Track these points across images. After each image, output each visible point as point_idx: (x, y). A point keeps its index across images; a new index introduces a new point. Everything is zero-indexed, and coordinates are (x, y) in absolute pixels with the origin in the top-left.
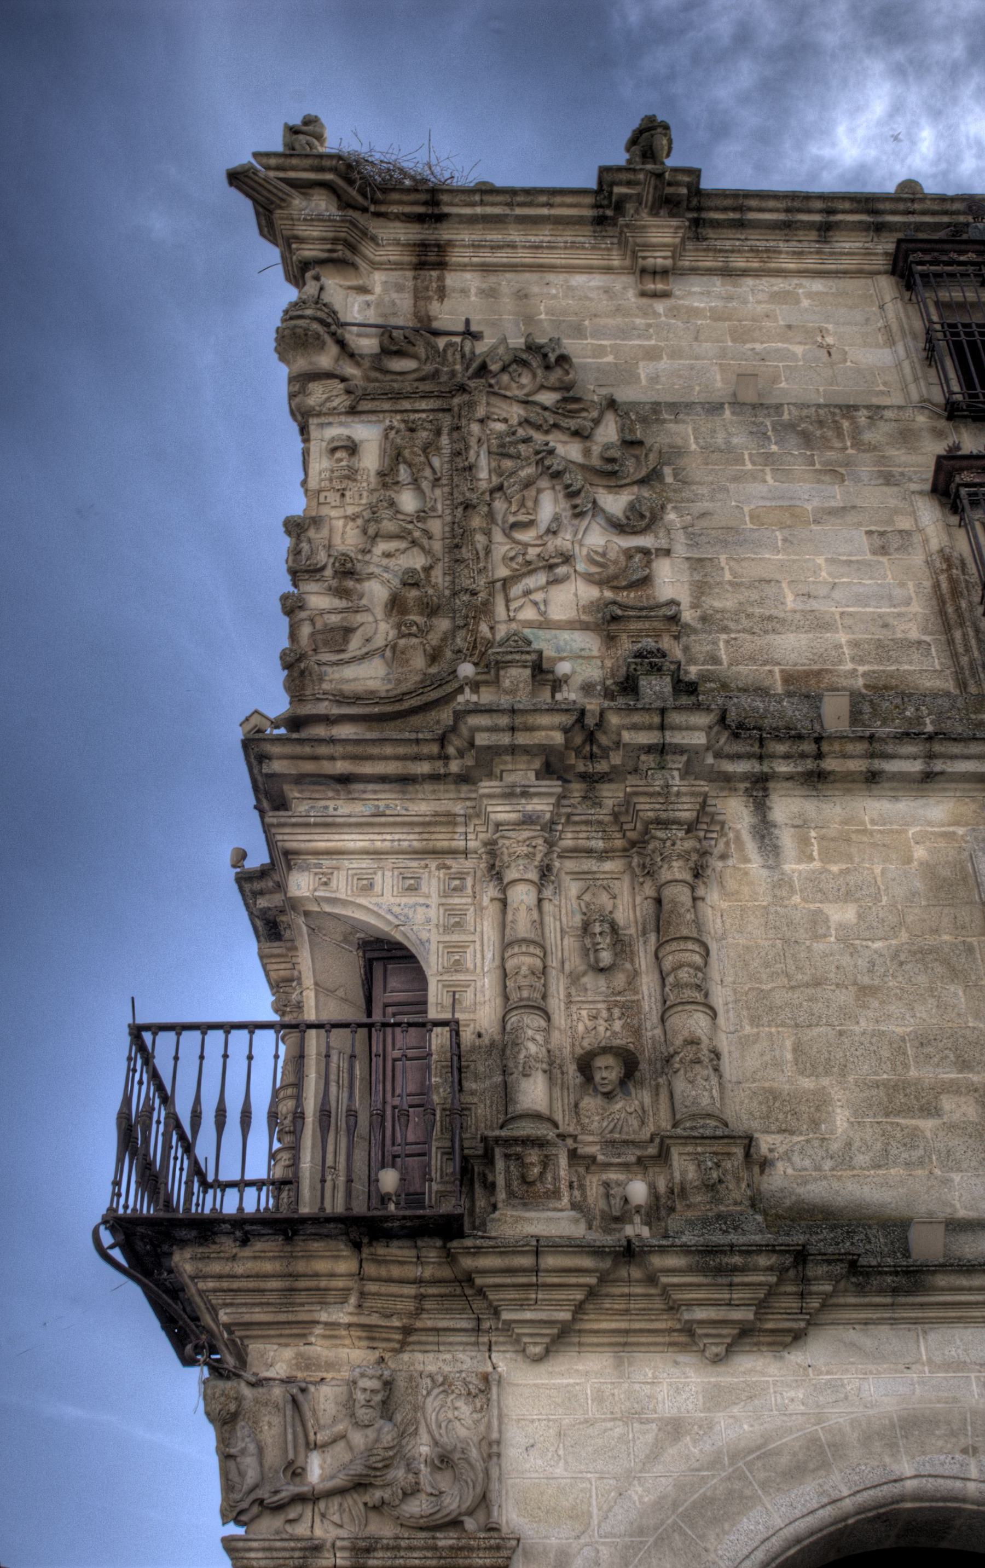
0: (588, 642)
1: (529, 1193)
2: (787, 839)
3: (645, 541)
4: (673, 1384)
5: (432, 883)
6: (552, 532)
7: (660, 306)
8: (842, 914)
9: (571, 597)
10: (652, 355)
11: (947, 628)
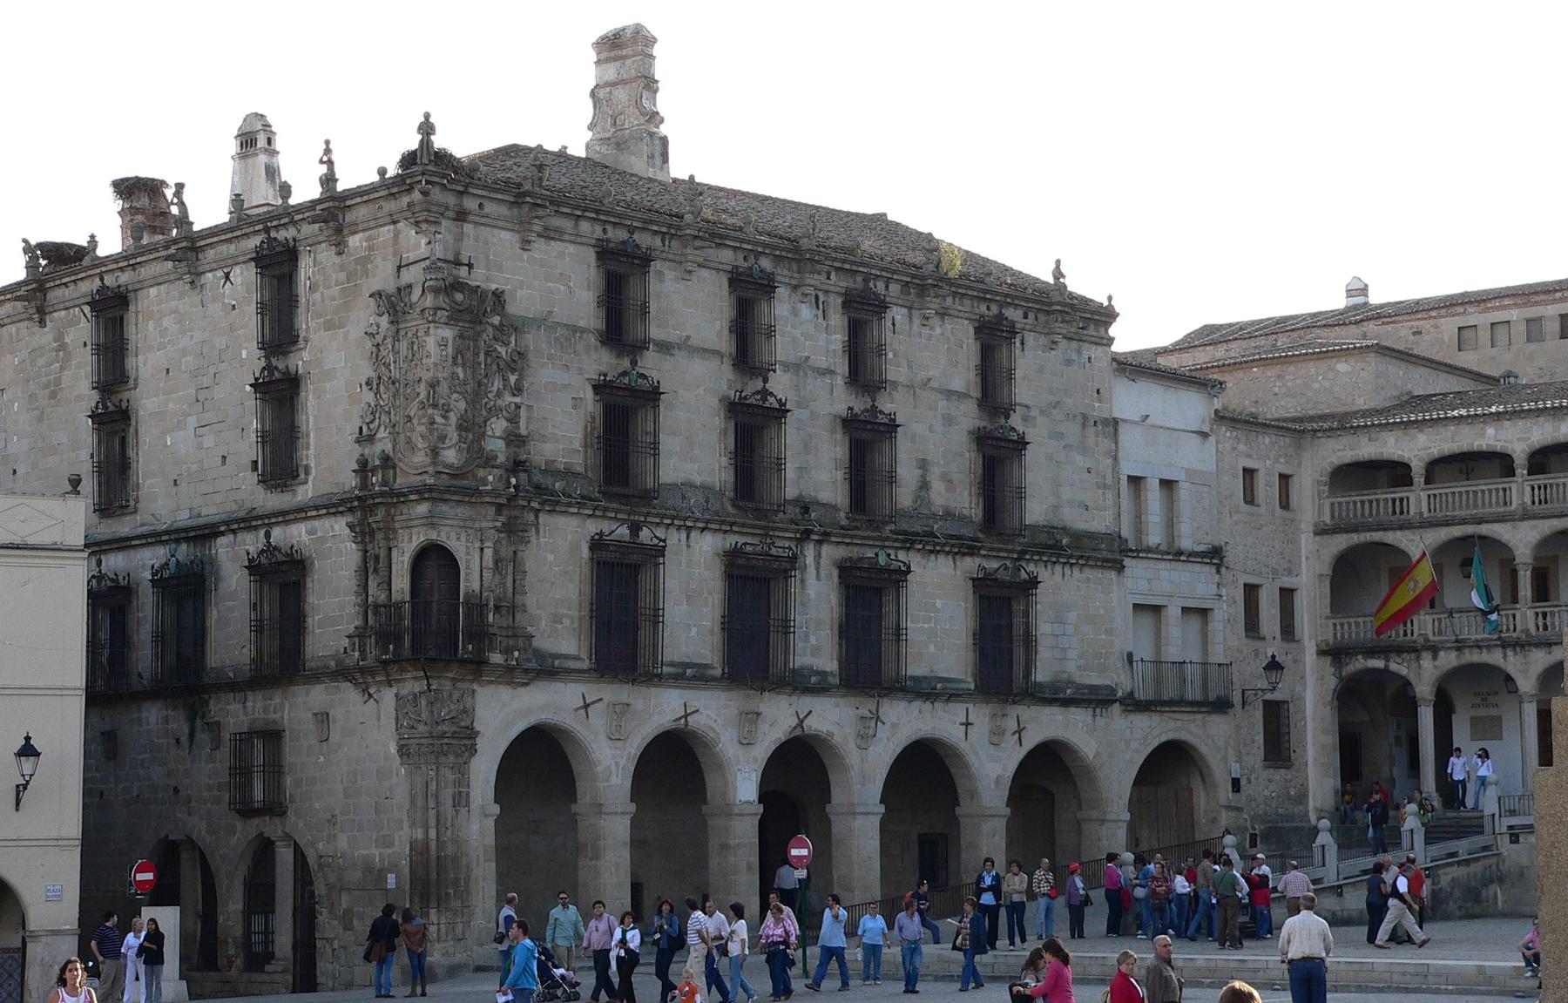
0: (501, 444)
1: (492, 650)
2: (541, 528)
3: (517, 400)
4: (505, 693)
5: (463, 538)
6: (499, 395)
7: (525, 255)
8: (551, 558)
9: (498, 426)
10: (521, 285)
11: (586, 446)
